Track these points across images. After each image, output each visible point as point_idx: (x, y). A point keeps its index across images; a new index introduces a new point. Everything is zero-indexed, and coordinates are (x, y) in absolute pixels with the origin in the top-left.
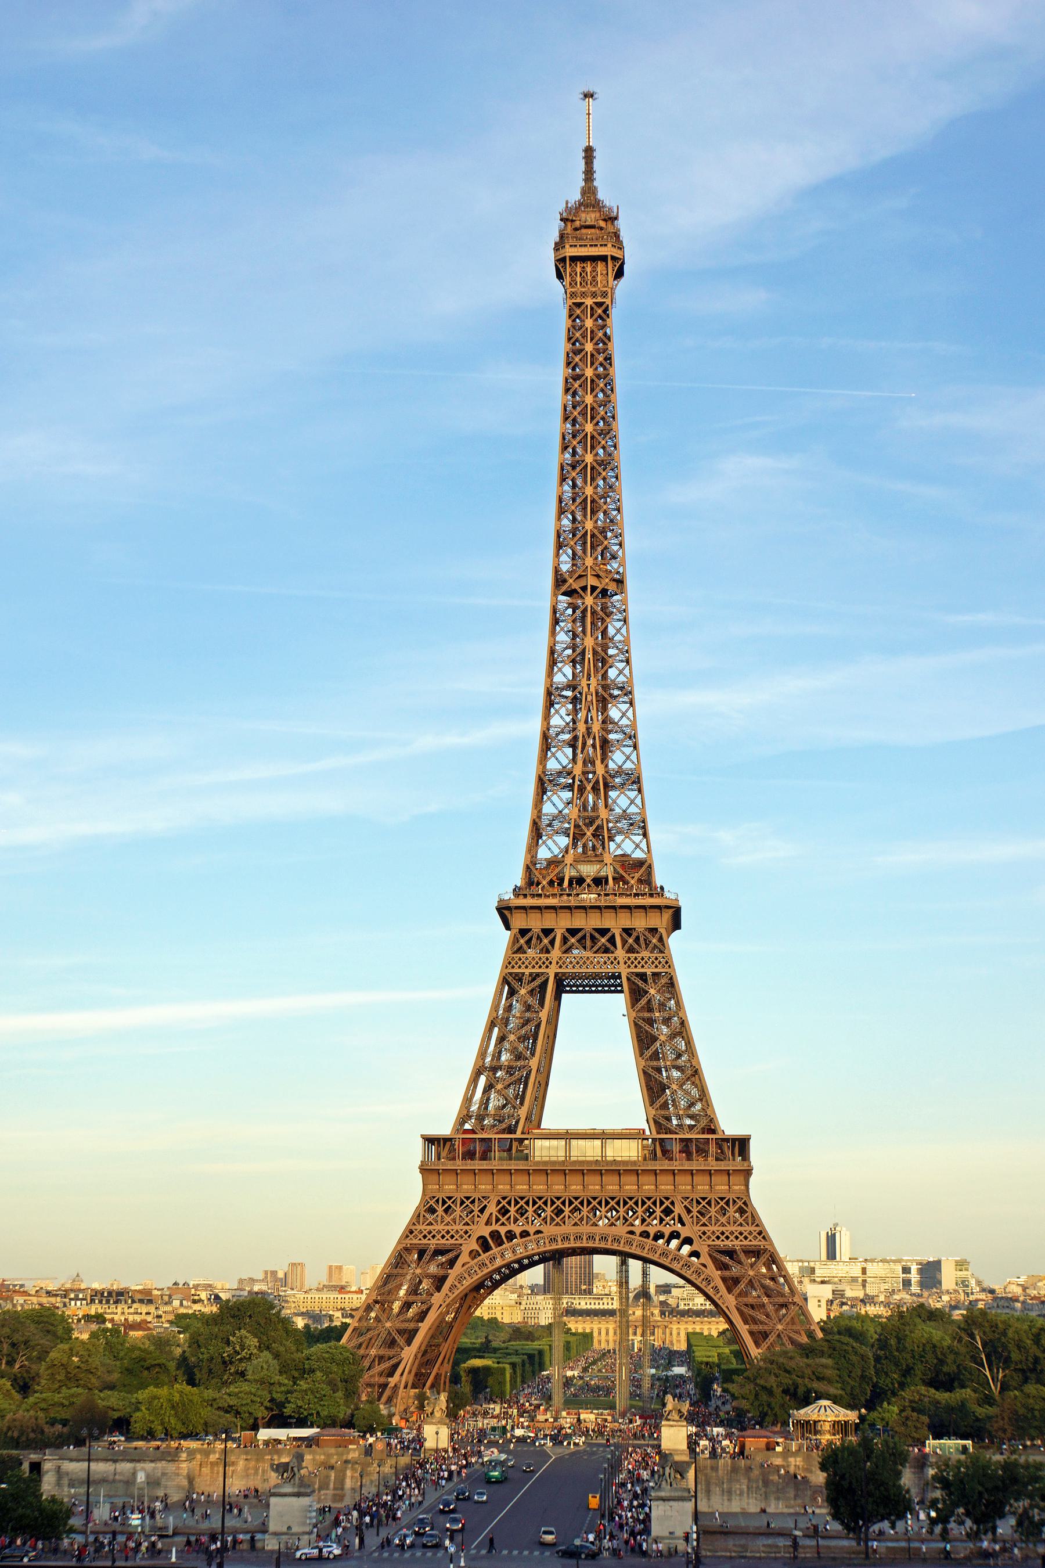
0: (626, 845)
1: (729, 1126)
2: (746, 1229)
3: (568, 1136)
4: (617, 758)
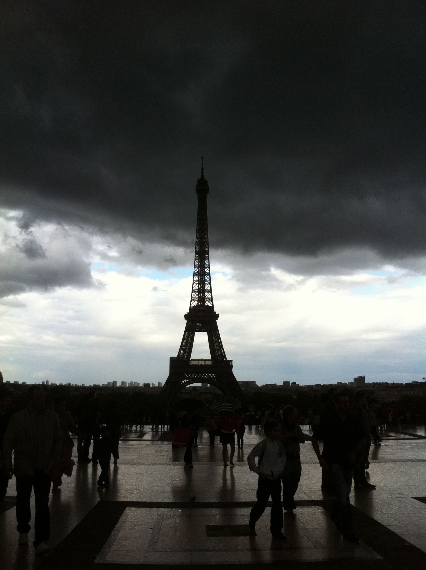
1: (228, 358)
3: (198, 360)
4: (207, 287)
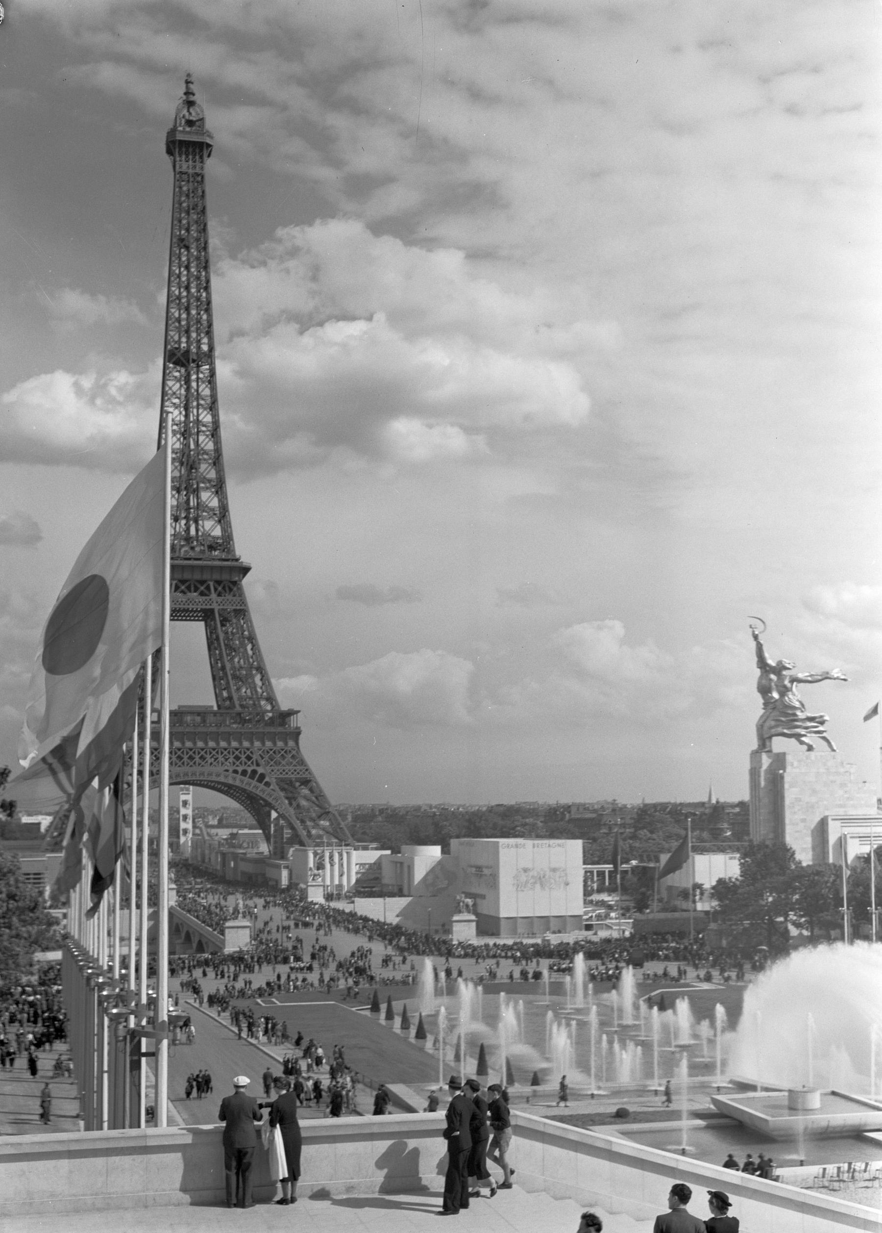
0: (211, 528)
1: (284, 706)
2: (299, 768)
